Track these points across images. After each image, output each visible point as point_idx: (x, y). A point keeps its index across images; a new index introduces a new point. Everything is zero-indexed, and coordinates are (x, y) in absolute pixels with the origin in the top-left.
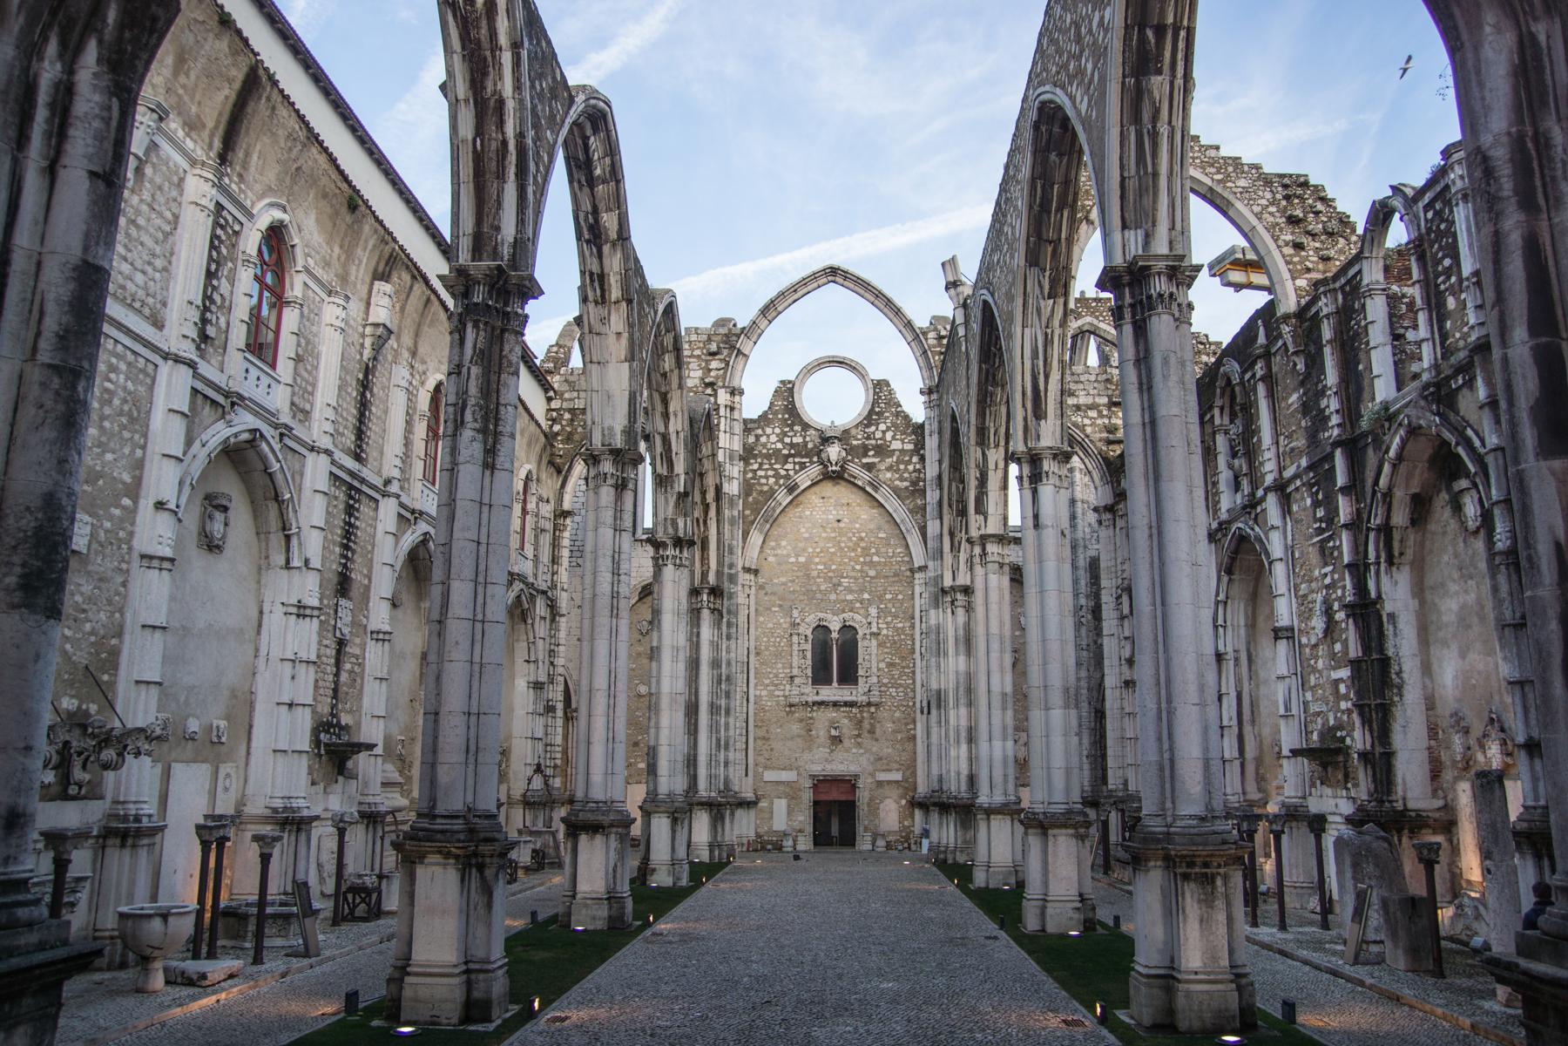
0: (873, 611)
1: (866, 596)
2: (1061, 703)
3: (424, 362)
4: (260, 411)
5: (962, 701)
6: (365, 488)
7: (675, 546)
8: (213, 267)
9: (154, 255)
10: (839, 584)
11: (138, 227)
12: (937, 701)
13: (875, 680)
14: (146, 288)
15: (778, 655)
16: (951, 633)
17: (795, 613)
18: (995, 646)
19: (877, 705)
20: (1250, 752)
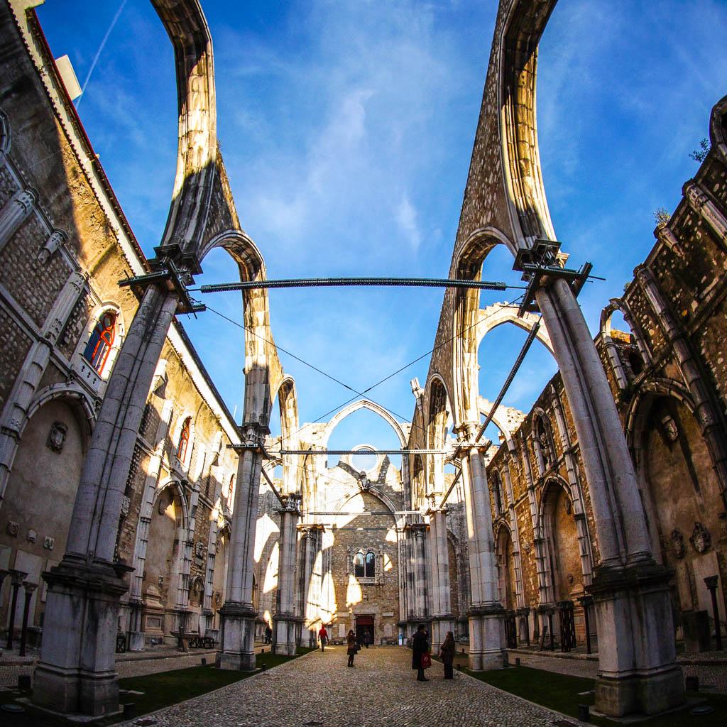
0: (381, 546)
1: (378, 540)
2: (487, 548)
3: (183, 406)
4: (86, 386)
5: (421, 576)
6: (143, 448)
7: (292, 498)
8: (75, 314)
9: (45, 295)
10: (367, 536)
11: (41, 280)
12: (411, 577)
13: (381, 575)
14: (36, 305)
15: (341, 565)
16: (415, 548)
17: (348, 547)
18: (440, 543)
19: (383, 585)
20: (557, 584)
